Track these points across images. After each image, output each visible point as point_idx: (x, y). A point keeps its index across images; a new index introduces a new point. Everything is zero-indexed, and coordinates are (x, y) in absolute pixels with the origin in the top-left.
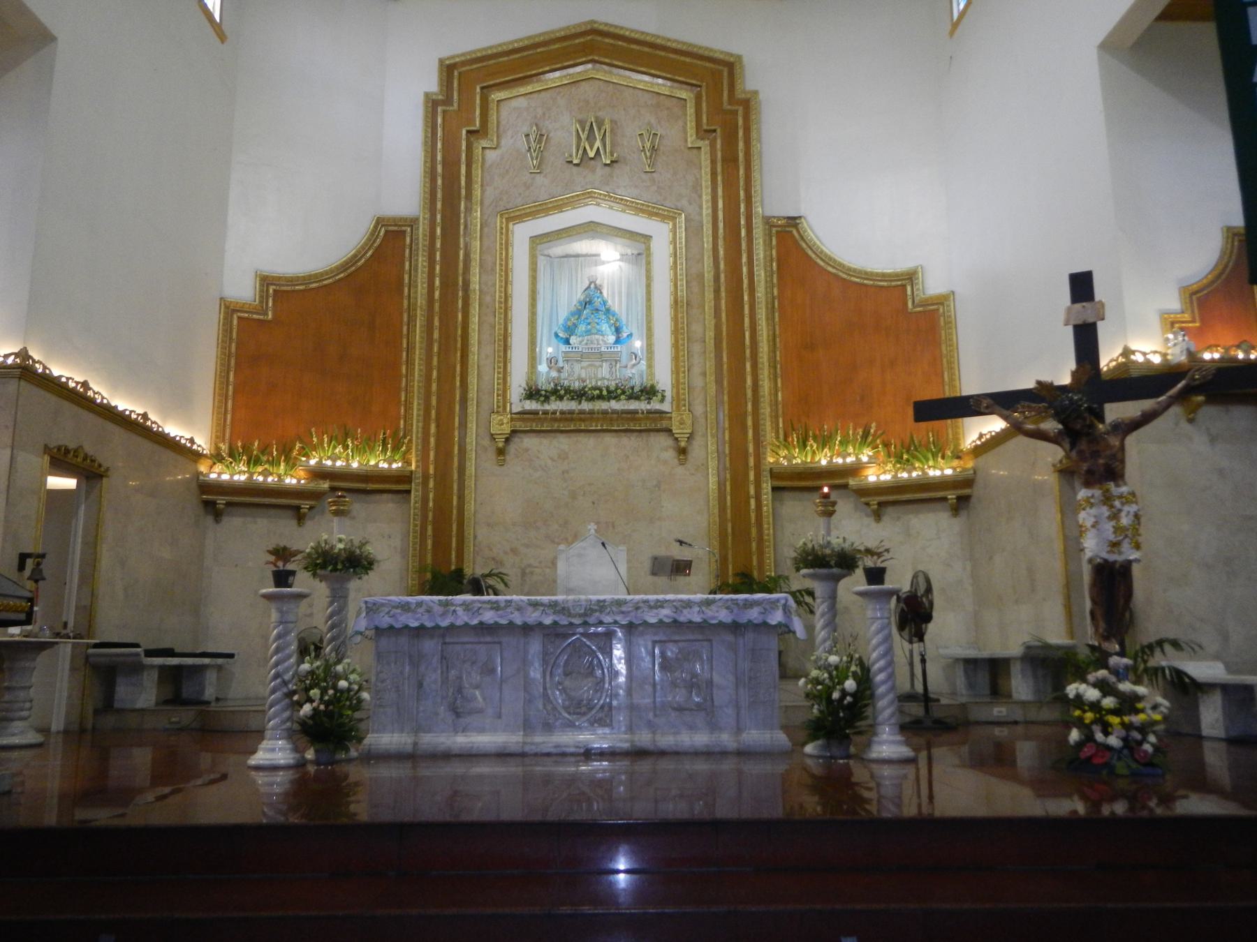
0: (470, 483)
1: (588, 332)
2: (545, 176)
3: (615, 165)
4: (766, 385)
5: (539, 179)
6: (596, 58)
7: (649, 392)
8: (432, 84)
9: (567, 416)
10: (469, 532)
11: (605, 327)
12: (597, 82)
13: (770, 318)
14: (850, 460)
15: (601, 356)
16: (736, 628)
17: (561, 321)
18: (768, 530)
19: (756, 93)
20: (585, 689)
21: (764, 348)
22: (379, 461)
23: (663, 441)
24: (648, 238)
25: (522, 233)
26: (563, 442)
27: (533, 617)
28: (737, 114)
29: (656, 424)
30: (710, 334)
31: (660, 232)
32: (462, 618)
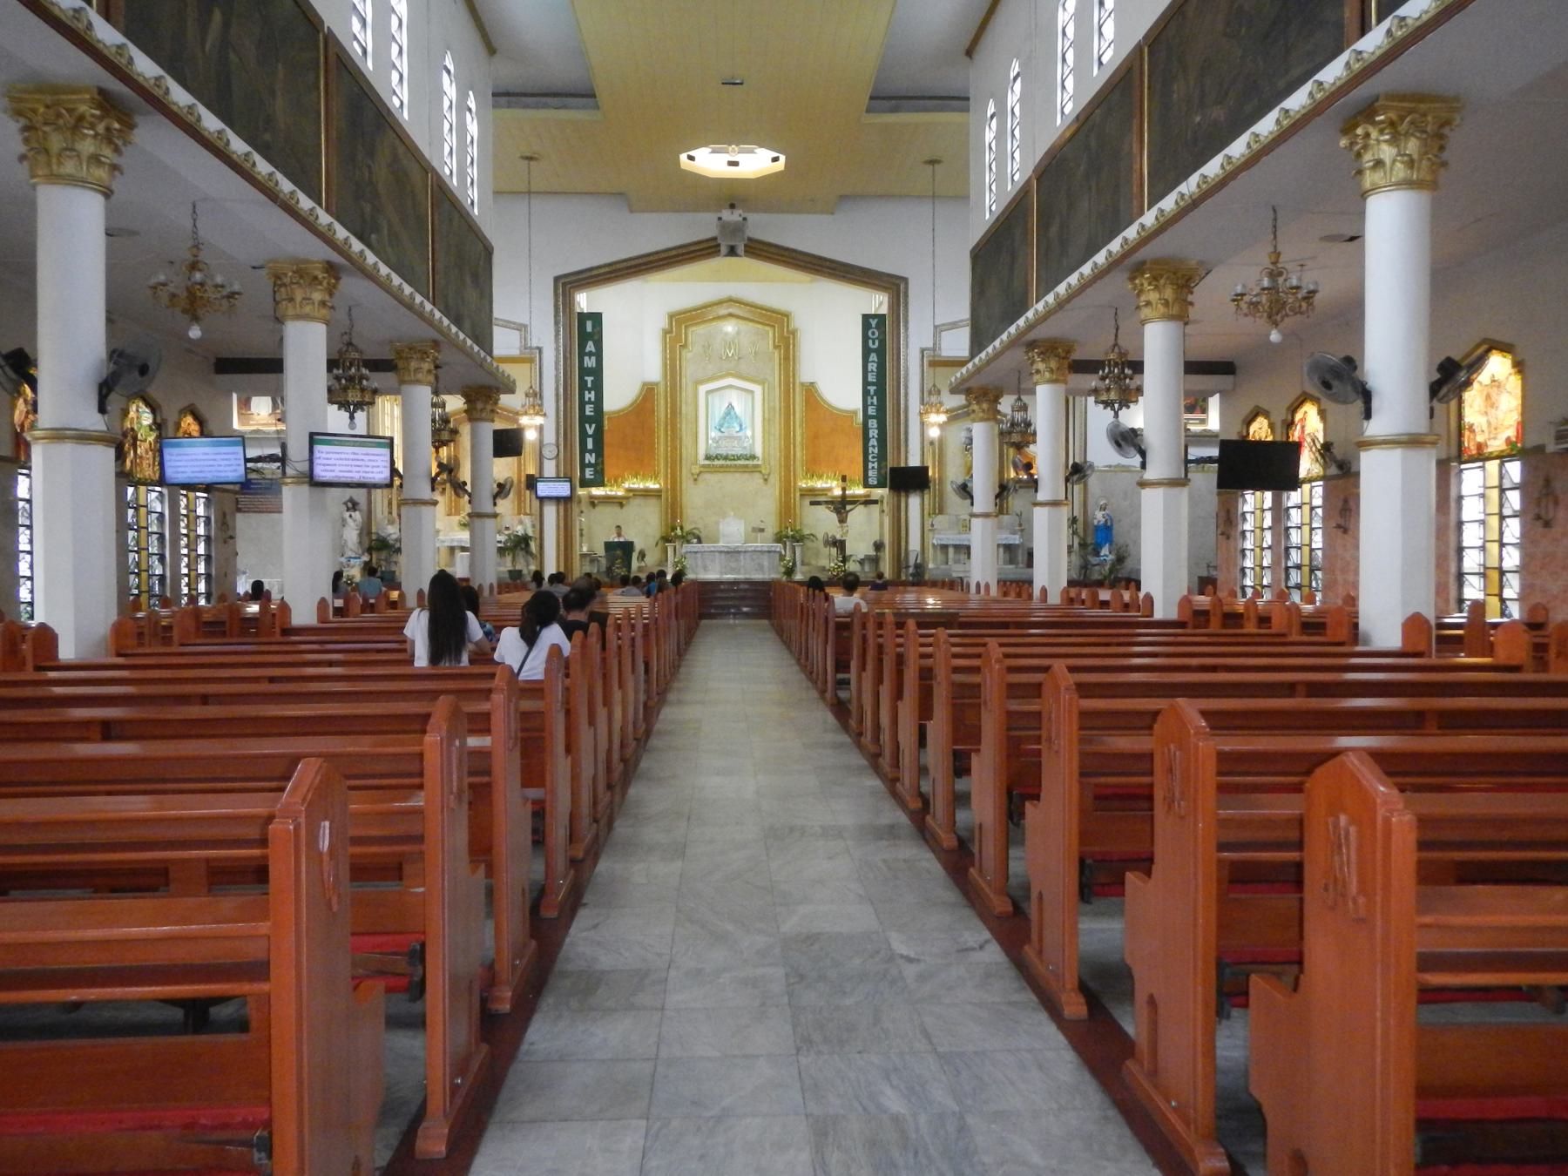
0: (684, 492)
1: (728, 427)
4: (799, 455)
7: (753, 457)
8: (664, 323)
9: (722, 466)
10: (684, 511)
11: (735, 425)
13: (801, 425)
14: (828, 485)
15: (731, 437)
16: (769, 552)
17: (717, 421)
18: (798, 511)
20: (733, 565)
21: (799, 439)
22: (652, 485)
23: (757, 475)
24: (752, 392)
25: (703, 389)
26: (719, 476)
27: (722, 549)
29: (756, 469)
30: (777, 433)
31: (757, 389)
32: (706, 549)
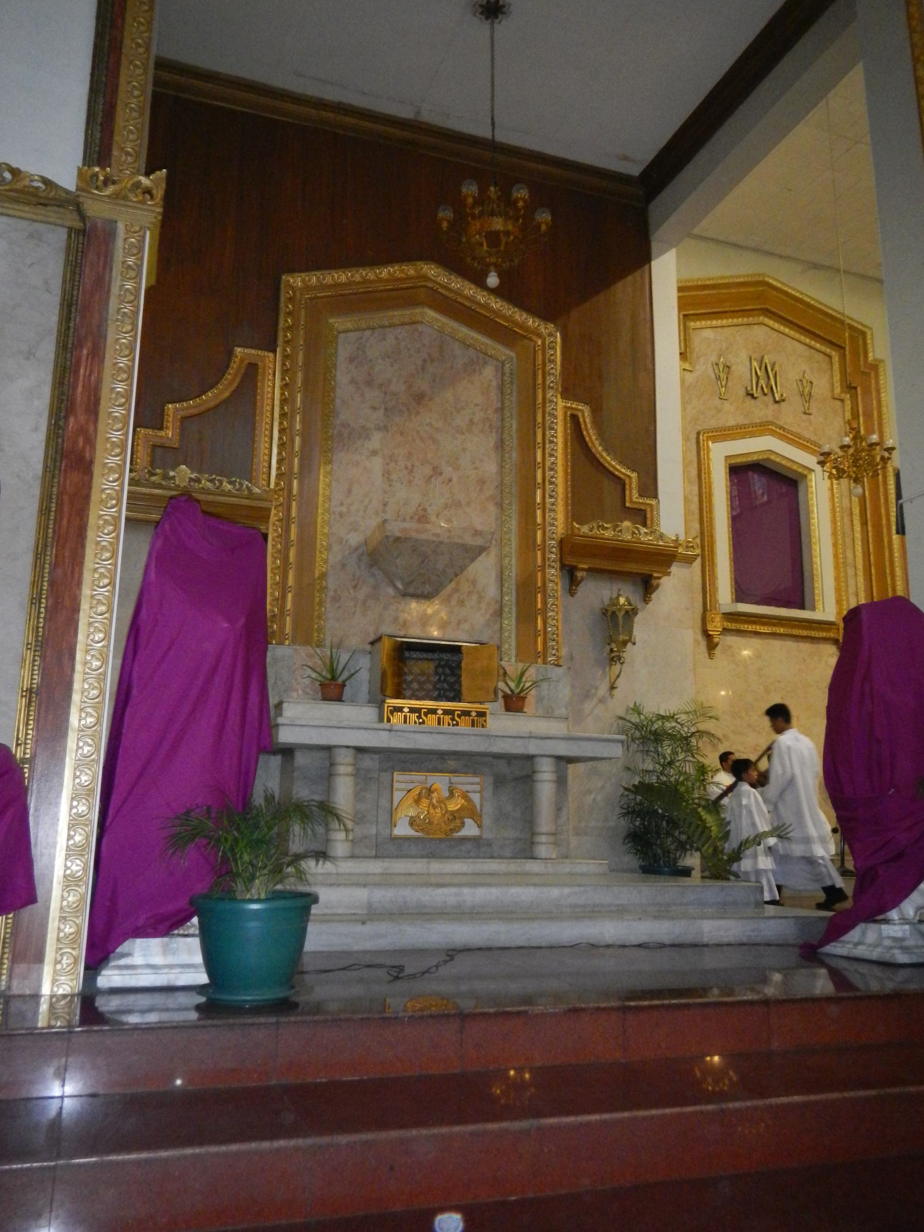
2: (731, 404)
3: (783, 404)
5: (727, 406)
6: (768, 307)
12: (765, 327)
19: (882, 361)
28: (870, 377)
